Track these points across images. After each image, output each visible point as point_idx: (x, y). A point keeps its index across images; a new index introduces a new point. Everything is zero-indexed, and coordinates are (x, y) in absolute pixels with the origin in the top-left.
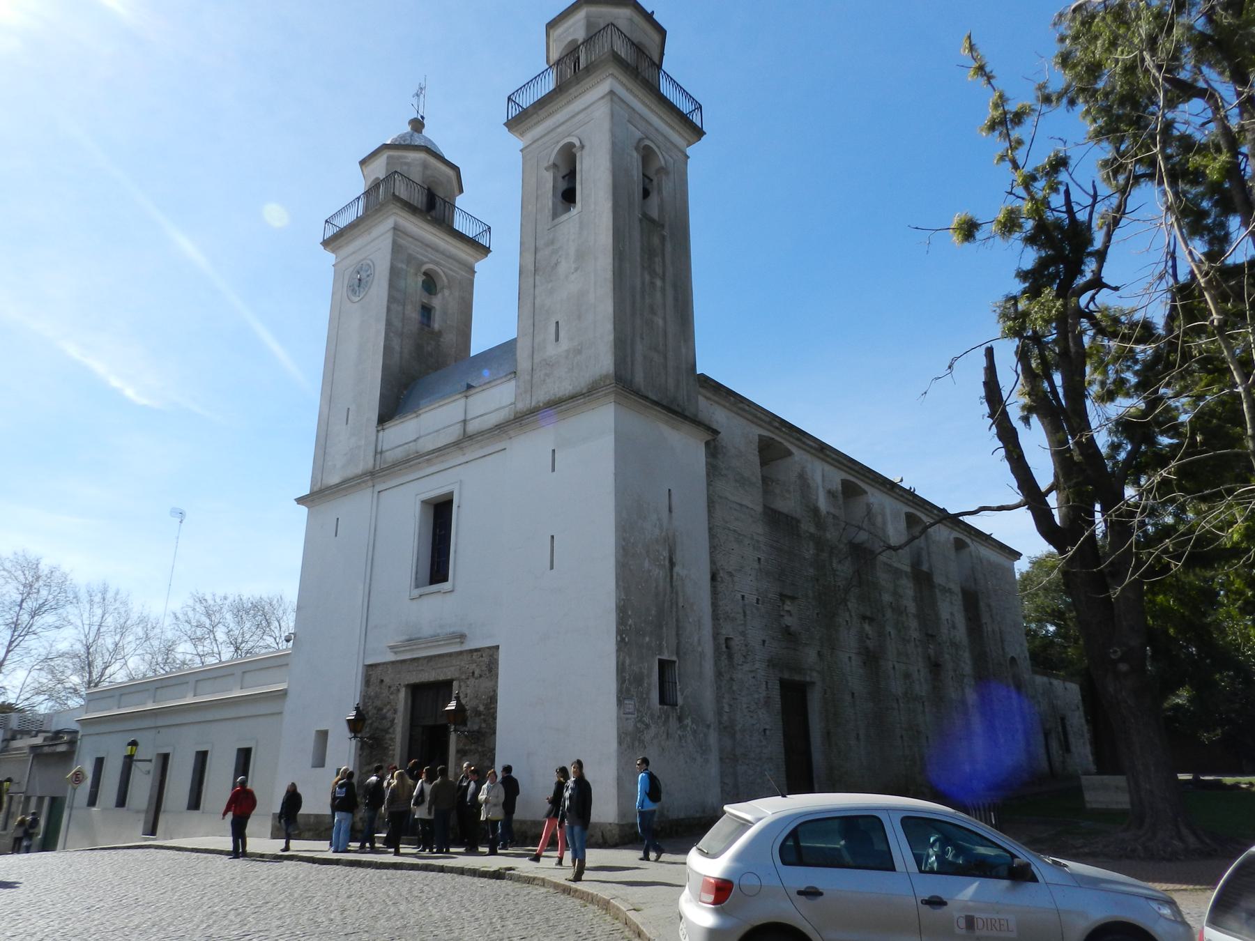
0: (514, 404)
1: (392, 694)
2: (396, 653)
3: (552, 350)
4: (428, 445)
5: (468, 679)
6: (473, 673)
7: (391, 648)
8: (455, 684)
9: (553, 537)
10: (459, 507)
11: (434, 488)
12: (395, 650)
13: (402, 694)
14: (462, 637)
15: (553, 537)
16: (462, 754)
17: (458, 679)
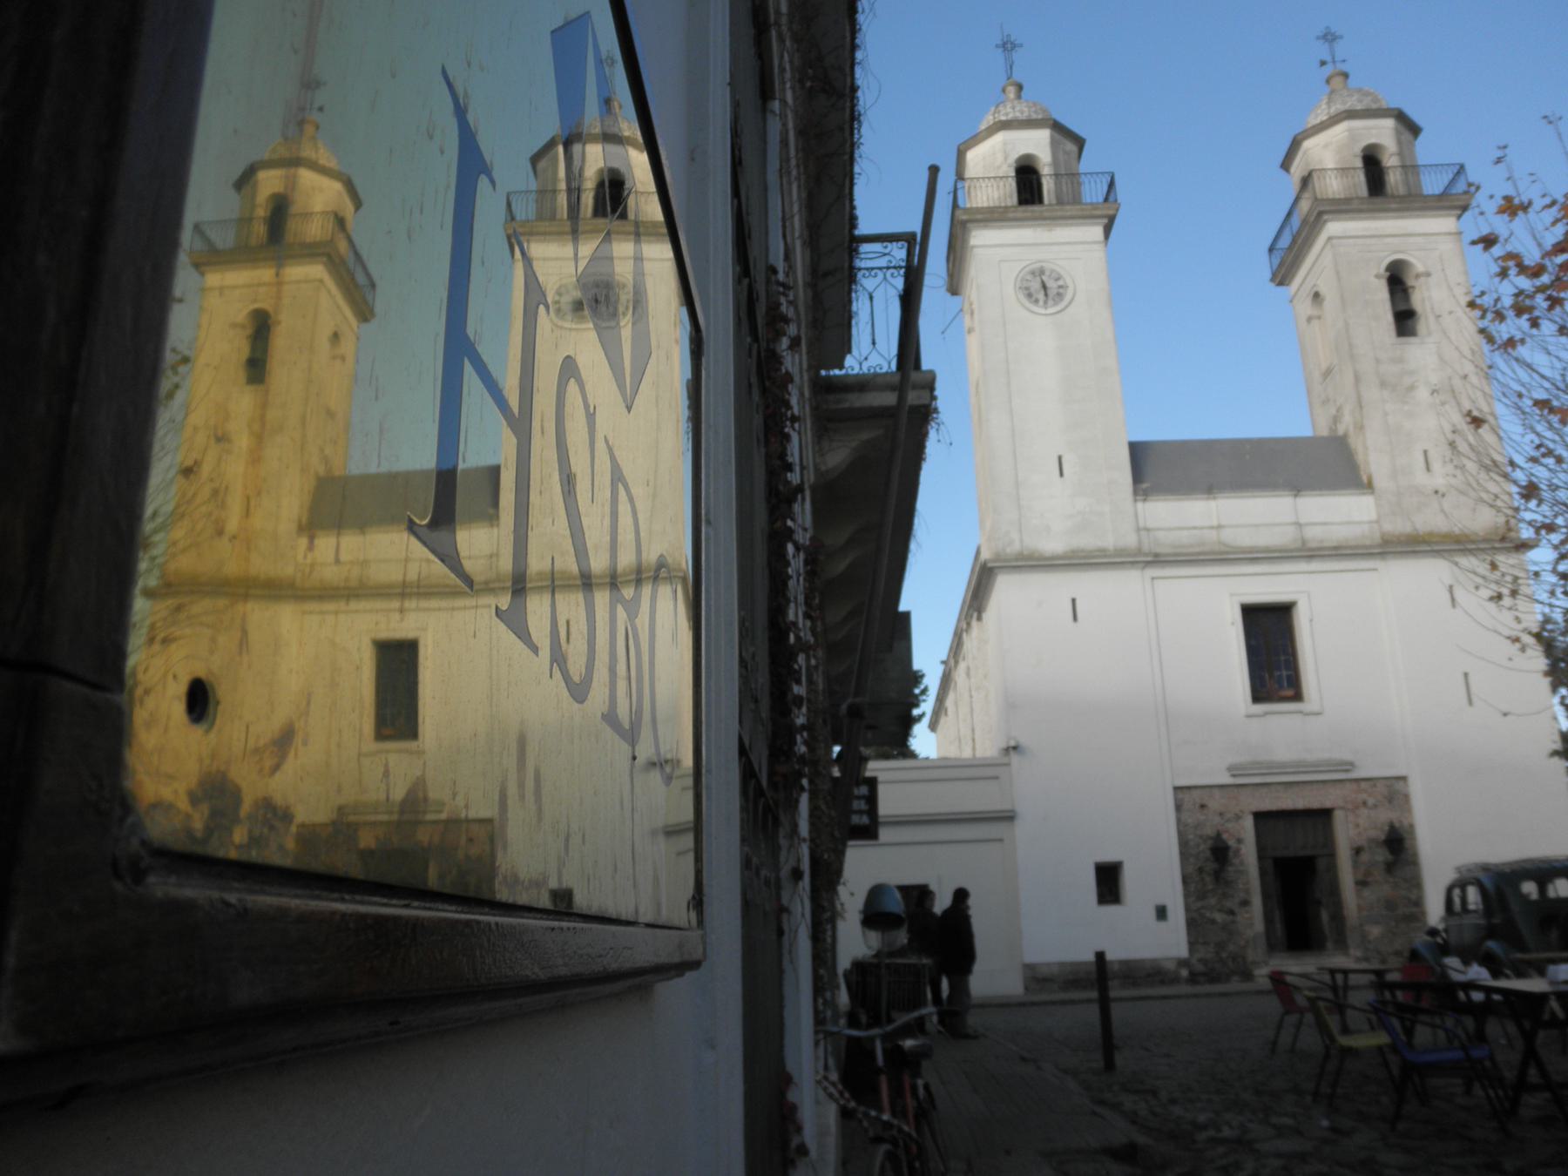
0: (1377, 522)
1: (1228, 821)
2: (1234, 776)
3: (1421, 478)
4: (1246, 539)
5: (1357, 808)
6: (1365, 803)
7: (1230, 769)
8: (1339, 816)
9: (1466, 675)
10: (1311, 620)
11: (1266, 588)
12: (1235, 772)
13: (1248, 823)
14: (1349, 766)
15: (1466, 675)
16: (1361, 884)
17: (1342, 808)
